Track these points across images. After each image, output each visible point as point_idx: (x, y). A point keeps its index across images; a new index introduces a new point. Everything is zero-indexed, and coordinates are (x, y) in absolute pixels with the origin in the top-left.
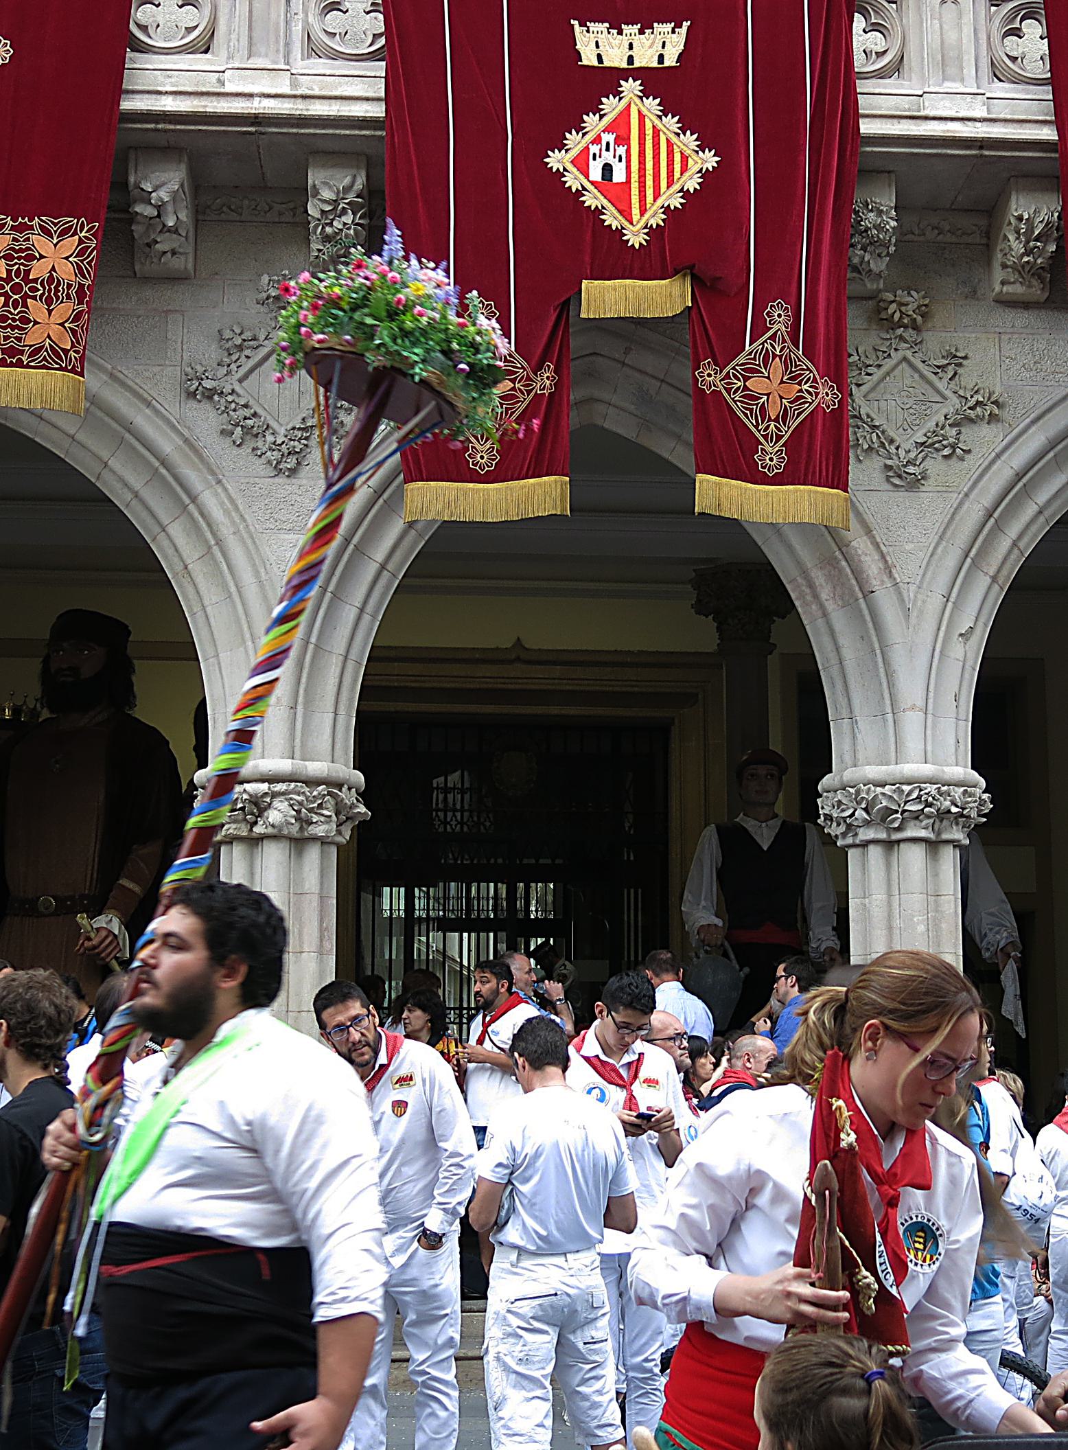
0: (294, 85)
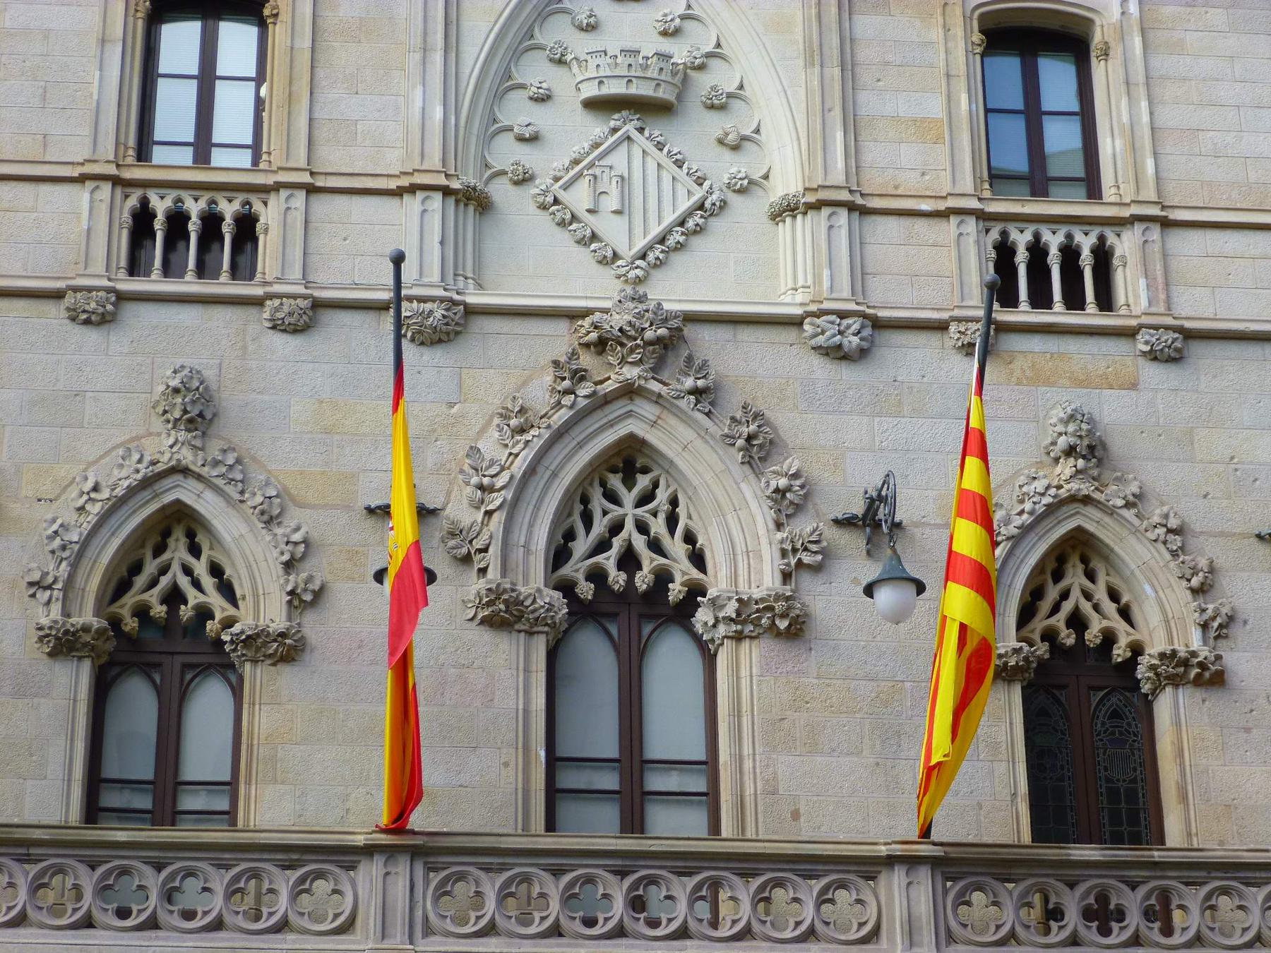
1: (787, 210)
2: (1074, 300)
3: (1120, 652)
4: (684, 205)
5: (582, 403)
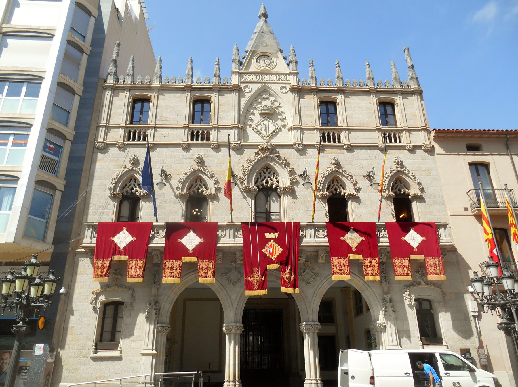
0: (235, 242)
1: (291, 129)
2: (334, 141)
3: (342, 194)
4: (275, 128)
5: (259, 158)
